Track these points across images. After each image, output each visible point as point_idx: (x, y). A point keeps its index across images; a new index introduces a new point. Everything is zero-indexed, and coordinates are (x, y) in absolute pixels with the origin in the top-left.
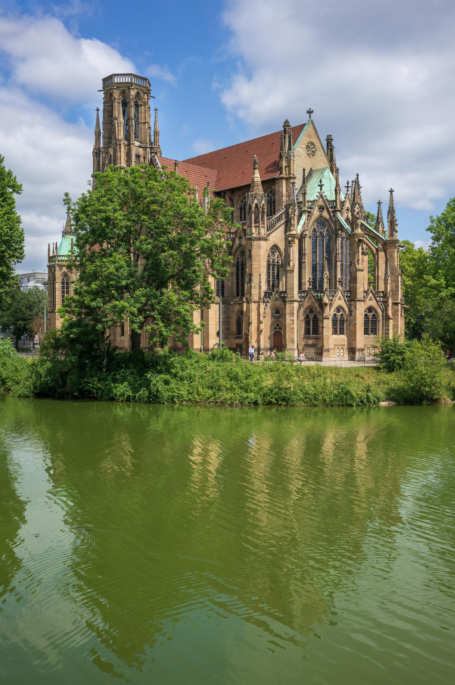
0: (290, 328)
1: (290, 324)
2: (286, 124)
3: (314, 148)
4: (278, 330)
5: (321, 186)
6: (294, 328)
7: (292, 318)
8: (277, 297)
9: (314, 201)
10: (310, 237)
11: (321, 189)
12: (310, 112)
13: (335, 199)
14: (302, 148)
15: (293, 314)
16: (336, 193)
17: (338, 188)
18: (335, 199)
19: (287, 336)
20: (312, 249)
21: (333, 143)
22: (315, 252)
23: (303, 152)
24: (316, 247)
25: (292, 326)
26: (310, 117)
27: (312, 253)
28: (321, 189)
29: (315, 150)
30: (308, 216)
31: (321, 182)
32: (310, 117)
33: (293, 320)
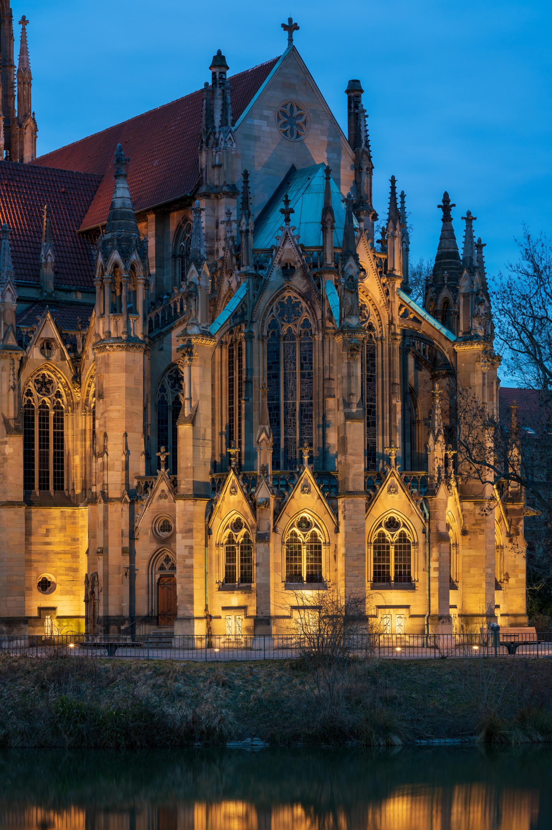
0: (185, 567)
1: (185, 557)
2: (219, 61)
3: (301, 115)
4: (167, 572)
5: (287, 213)
6: (191, 567)
7: (188, 542)
8: (163, 491)
9: (271, 250)
10: (261, 338)
11: (287, 220)
12: (291, 27)
13: (321, 244)
14: (266, 118)
15: (190, 531)
16: (324, 229)
17: (329, 216)
18: (321, 244)
19: (178, 587)
20: (269, 368)
21: (365, 101)
22: (276, 376)
23: (268, 129)
24: (278, 363)
25: (188, 562)
26: (290, 40)
27: (269, 378)
28: (287, 220)
29: (305, 123)
30: (257, 286)
31: (287, 202)
32: (290, 40)
33: (191, 548)
